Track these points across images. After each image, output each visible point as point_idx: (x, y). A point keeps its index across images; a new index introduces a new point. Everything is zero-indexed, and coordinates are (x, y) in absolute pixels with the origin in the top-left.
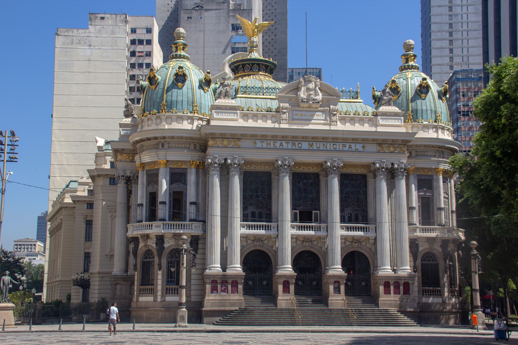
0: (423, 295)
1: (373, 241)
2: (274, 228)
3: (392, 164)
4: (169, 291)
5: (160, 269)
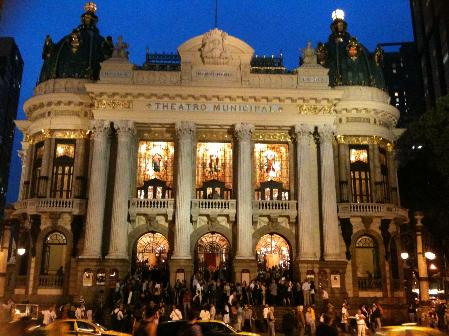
0: (359, 287)
1: (295, 221)
2: (170, 205)
3: (316, 128)
4: (43, 282)
5: (34, 255)
